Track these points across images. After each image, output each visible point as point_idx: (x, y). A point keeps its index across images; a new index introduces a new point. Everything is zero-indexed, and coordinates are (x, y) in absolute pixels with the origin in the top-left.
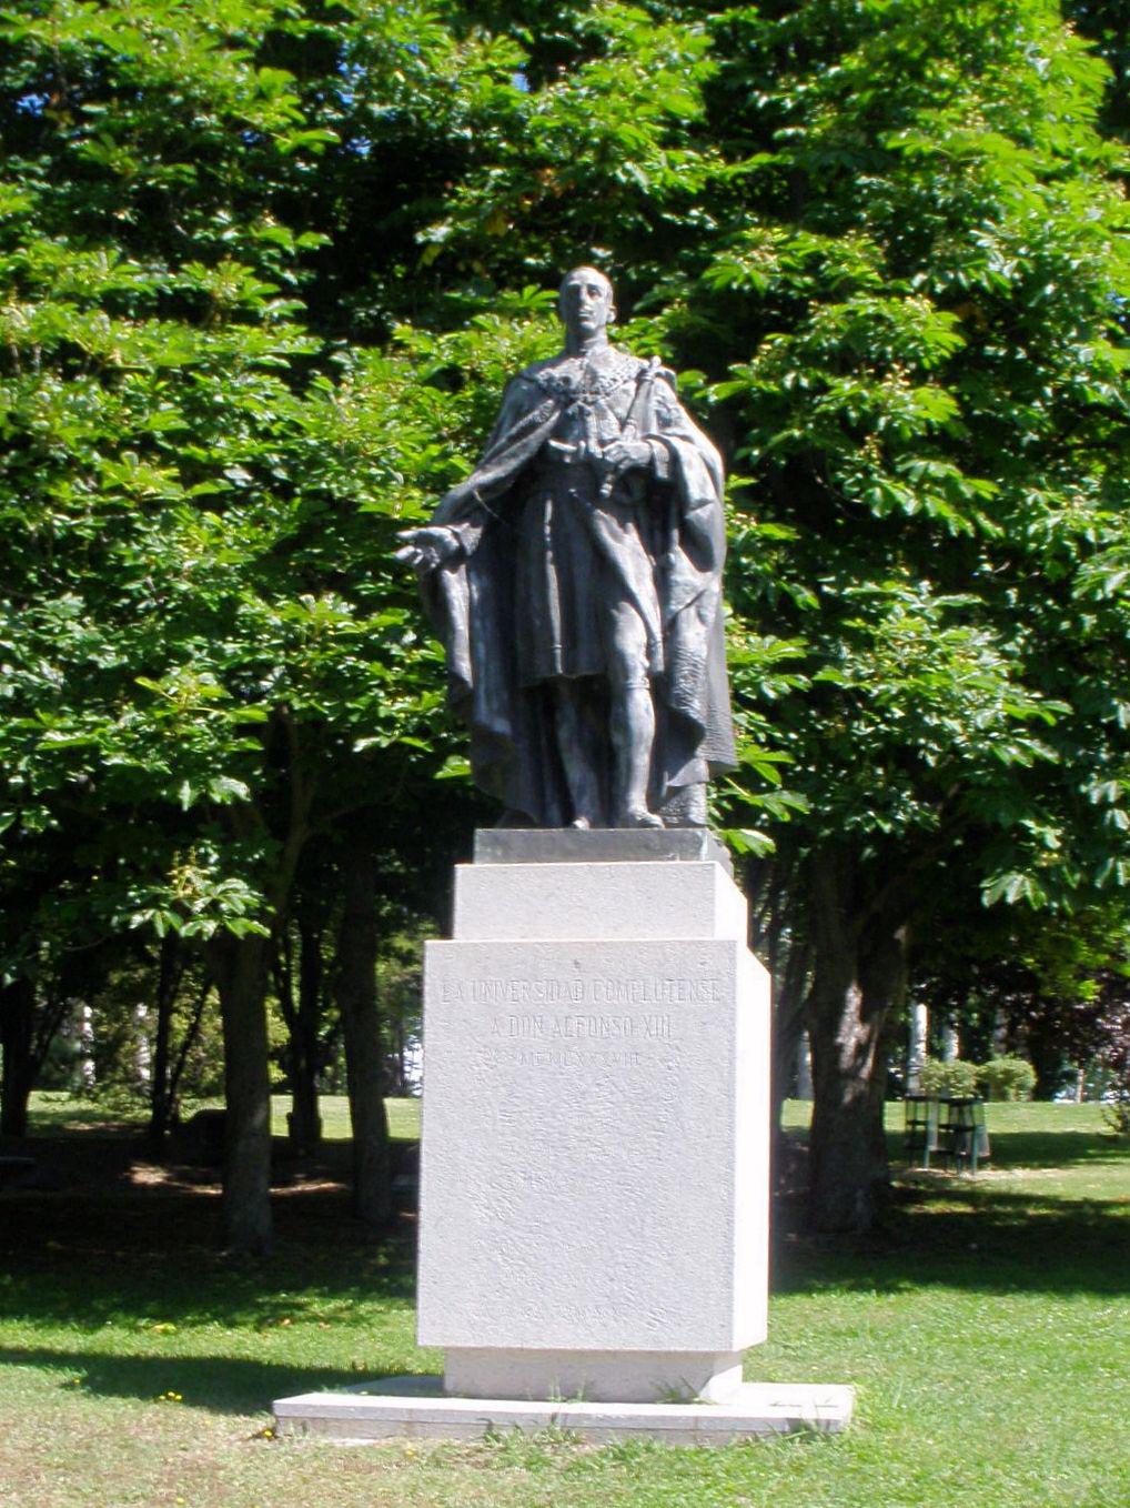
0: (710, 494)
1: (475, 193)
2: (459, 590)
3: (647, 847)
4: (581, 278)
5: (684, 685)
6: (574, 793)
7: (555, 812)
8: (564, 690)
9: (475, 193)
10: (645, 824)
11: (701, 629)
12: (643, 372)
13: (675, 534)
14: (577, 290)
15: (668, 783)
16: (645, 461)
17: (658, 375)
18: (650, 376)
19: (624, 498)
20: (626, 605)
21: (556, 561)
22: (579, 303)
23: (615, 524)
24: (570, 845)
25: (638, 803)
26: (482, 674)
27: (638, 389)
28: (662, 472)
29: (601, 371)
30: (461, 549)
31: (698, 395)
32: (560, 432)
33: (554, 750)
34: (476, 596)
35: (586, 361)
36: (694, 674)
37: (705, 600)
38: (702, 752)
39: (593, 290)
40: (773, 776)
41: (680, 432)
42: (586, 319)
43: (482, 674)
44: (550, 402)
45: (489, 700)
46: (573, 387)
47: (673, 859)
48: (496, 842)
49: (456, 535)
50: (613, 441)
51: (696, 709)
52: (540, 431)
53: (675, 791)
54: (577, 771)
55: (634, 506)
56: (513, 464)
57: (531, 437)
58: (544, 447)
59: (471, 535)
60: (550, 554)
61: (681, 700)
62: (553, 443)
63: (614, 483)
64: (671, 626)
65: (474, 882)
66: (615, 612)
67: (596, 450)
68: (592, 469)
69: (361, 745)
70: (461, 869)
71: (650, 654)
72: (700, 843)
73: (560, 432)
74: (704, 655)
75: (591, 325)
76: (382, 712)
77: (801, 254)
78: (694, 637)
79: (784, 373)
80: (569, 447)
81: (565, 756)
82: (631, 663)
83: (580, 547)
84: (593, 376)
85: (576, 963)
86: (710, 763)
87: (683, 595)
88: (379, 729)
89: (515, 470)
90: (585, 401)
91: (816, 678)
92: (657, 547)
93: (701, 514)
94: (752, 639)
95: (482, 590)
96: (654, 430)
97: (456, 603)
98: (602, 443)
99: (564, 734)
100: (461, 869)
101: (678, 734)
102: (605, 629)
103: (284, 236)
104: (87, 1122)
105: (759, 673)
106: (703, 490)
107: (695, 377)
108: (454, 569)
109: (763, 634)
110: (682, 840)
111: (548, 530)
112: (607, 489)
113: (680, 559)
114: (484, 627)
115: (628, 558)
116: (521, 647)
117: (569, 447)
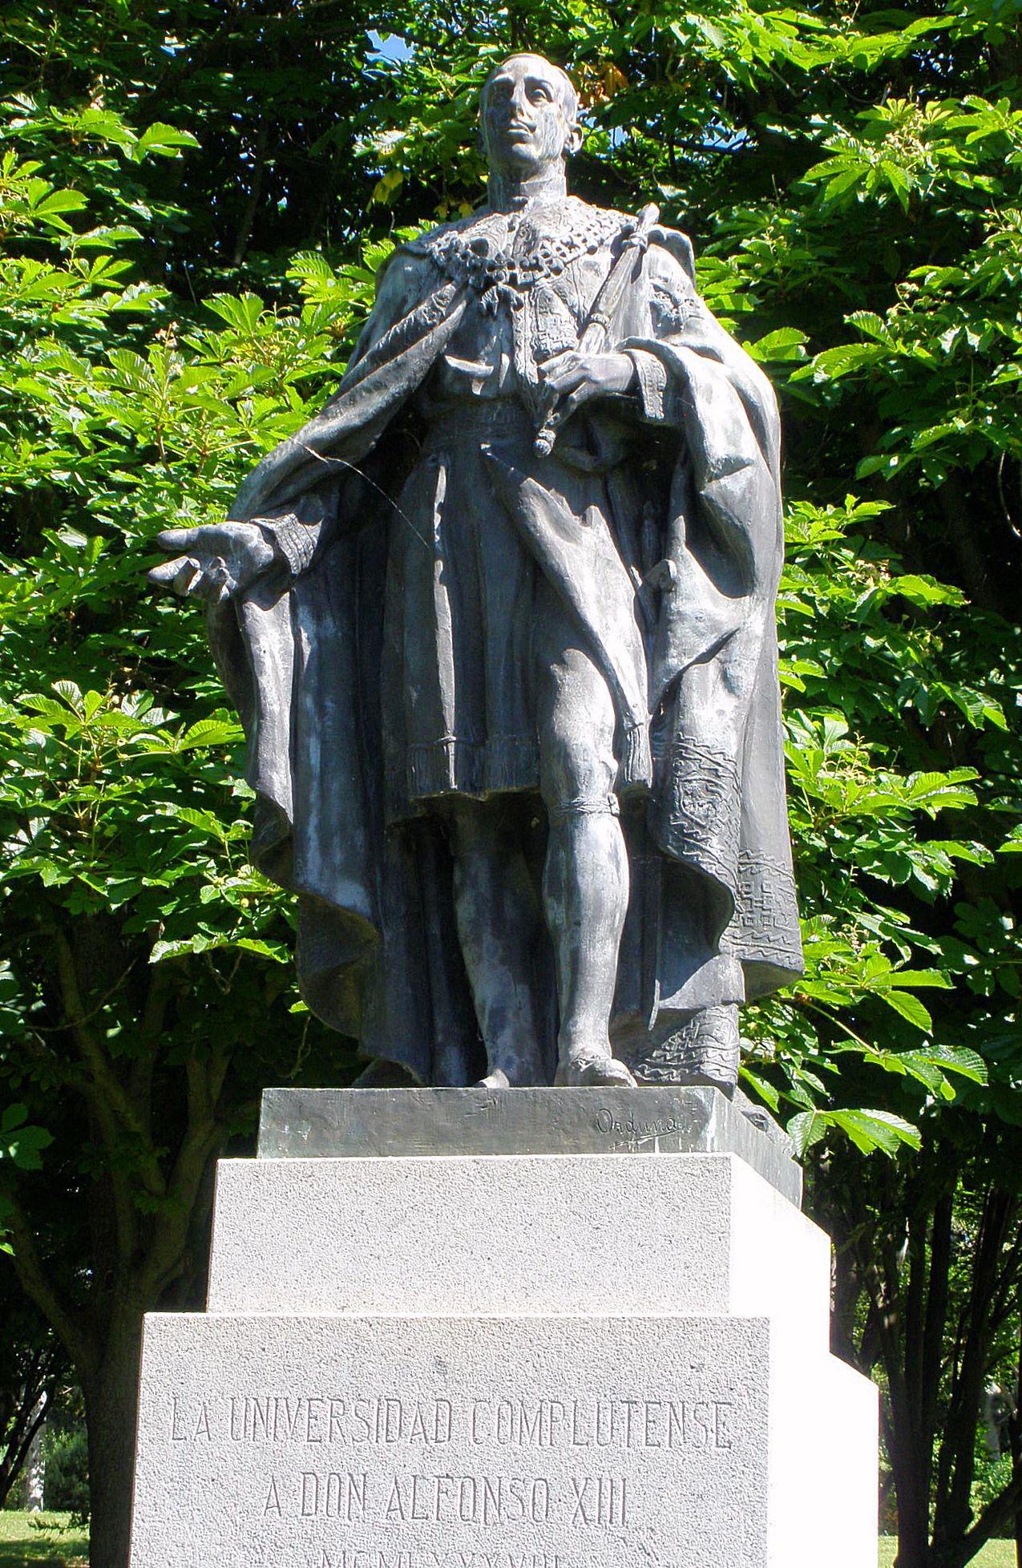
0: (748, 447)
1: (451, 80)
2: (275, 638)
3: (596, 1125)
4: (514, 68)
5: (692, 808)
6: (484, 1024)
7: (452, 1060)
8: (465, 823)
9: (451, 80)
10: (595, 1077)
11: (727, 703)
12: (627, 232)
13: (681, 525)
14: (508, 87)
15: (659, 1004)
16: (623, 385)
17: (655, 238)
18: (640, 236)
19: (585, 460)
20: (578, 656)
21: (453, 581)
22: (511, 111)
23: (564, 508)
24: (442, 1120)
25: (591, 1037)
26: (313, 797)
27: (614, 263)
28: (654, 408)
29: (544, 230)
30: (280, 562)
31: (796, 375)
32: (463, 342)
33: (438, 946)
34: (307, 650)
35: (522, 216)
36: (711, 788)
37: (736, 647)
38: (729, 940)
39: (535, 89)
40: (919, 1016)
41: (696, 341)
42: (521, 139)
43: (313, 797)
44: (449, 289)
45: (325, 848)
46: (490, 257)
47: (649, 1147)
48: (300, 1113)
49: (270, 536)
50: (561, 351)
51: (716, 856)
52: (429, 339)
53: (681, 1020)
54: (489, 982)
55: (603, 475)
56: (378, 401)
57: (413, 350)
58: (437, 367)
59: (299, 539)
60: (440, 566)
61: (684, 838)
62: (453, 362)
63: (561, 431)
64: (668, 698)
65: (250, 1197)
66: (555, 668)
67: (527, 367)
68: (521, 402)
69: (161, 950)
70: (228, 1169)
71: (621, 747)
72: (704, 1118)
73: (463, 342)
74: (732, 751)
75: (531, 150)
76: (207, 895)
77: (971, 139)
78: (713, 718)
79: (939, 328)
80: (481, 368)
81: (468, 954)
82: (581, 764)
83: (496, 553)
84: (530, 238)
85: (440, 1363)
86: (746, 965)
87: (693, 639)
88: (202, 925)
89: (381, 412)
90: (513, 281)
91: (1004, 849)
92: (644, 550)
93: (733, 485)
94: (883, 776)
95: (319, 640)
96: (647, 333)
97: (267, 660)
98: (540, 356)
99: (465, 910)
100: (228, 1169)
101: (679, 906)
102: (538, 698)
103: (123, 136)
104: (43, 1551)
105: (897, 837)
106: (733, 441)
107: (788, 340)
108: (268, 603)
109: (904, 769)
110: (664, 1110)
111: (437, 519)
112: (546, 439)
113: (689, 573)
114: (321, 708)
115: (587, 571)
116: (390, 747)
117: (481, 368)
